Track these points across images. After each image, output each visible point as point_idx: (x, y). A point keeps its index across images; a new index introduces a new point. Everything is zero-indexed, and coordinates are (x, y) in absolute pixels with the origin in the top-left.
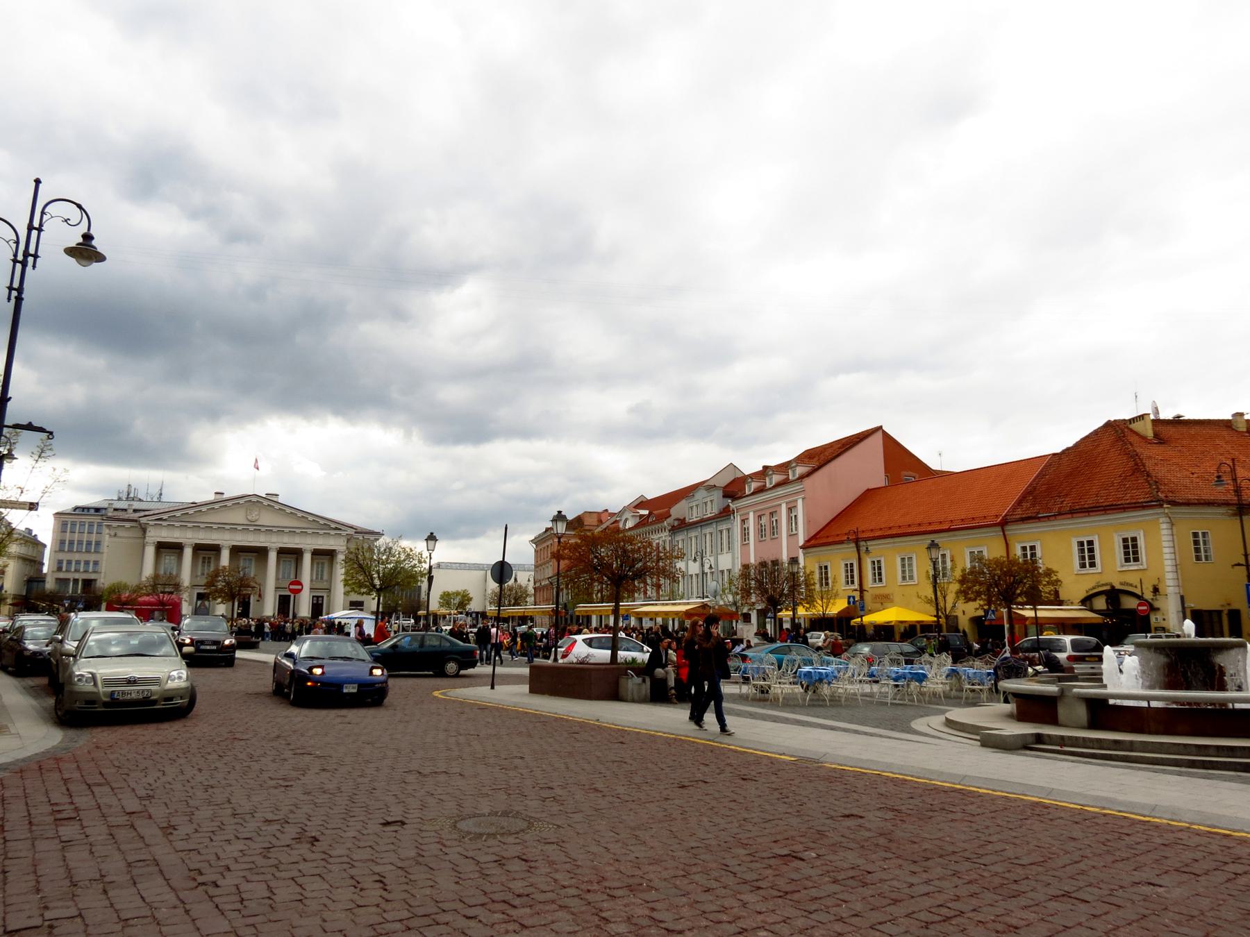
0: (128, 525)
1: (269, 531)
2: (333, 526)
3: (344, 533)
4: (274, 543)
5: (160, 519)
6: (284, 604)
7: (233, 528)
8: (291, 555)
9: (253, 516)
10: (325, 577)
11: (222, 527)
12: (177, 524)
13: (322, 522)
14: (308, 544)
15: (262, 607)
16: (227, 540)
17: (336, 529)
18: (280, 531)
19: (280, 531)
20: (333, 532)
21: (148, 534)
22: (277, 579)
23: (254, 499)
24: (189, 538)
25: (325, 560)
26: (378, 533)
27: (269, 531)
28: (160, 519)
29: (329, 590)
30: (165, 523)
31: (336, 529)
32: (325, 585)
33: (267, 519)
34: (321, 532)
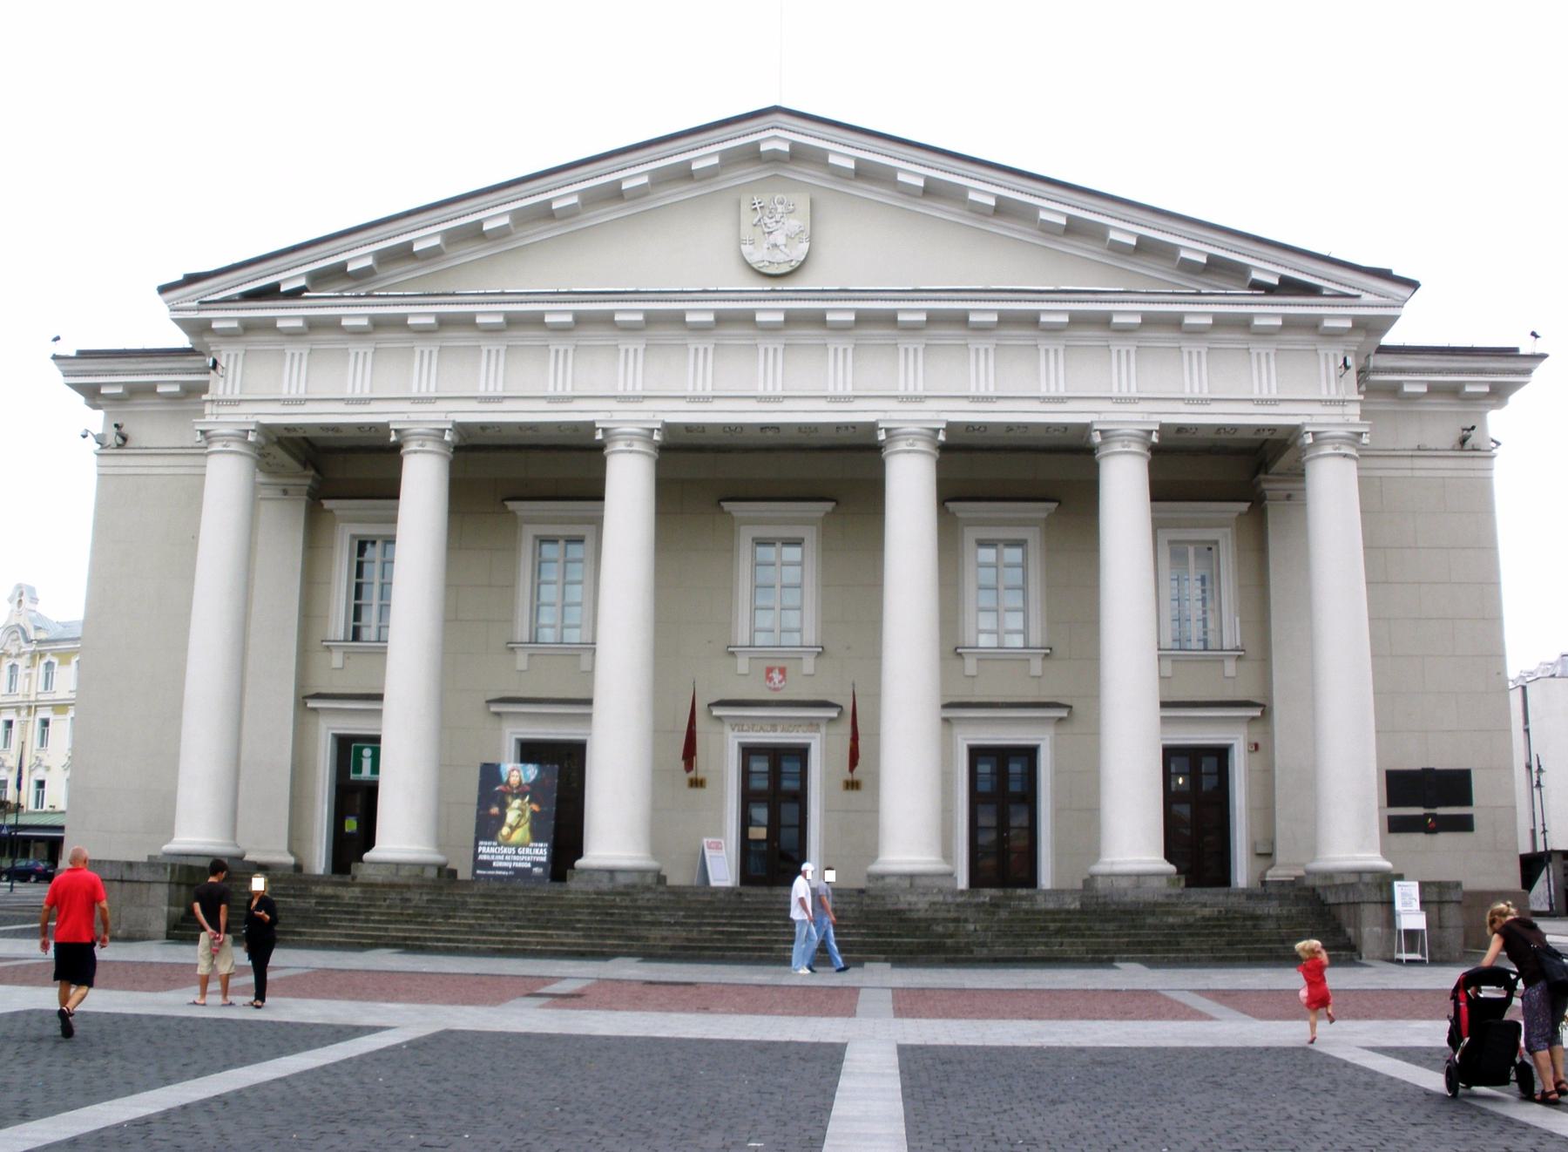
1: (876, 323)
2: (1267, 271)
3: (1337, 316)
4: (914, 398)
5: (270, 293)
6: (1002, 793)
9: (779, 243)
12: (355, 314)
14: (1124, 396)
15: (864, 830)
16: (630, 396)
17: (1289, 287)
20: (1269, 312)
21: (219, 387)
22: (952, 650)
23: (775, 140)
24: (421, 394)
25: (1219, 522)
26: (1510, 353)
27: (876, 323)
28: (270, 293)
29: (1259, 709)
30: (289, 315)
31: (1289, 287)
32: (1234, 680)
33: (867, 254)
34: (1199, 313)
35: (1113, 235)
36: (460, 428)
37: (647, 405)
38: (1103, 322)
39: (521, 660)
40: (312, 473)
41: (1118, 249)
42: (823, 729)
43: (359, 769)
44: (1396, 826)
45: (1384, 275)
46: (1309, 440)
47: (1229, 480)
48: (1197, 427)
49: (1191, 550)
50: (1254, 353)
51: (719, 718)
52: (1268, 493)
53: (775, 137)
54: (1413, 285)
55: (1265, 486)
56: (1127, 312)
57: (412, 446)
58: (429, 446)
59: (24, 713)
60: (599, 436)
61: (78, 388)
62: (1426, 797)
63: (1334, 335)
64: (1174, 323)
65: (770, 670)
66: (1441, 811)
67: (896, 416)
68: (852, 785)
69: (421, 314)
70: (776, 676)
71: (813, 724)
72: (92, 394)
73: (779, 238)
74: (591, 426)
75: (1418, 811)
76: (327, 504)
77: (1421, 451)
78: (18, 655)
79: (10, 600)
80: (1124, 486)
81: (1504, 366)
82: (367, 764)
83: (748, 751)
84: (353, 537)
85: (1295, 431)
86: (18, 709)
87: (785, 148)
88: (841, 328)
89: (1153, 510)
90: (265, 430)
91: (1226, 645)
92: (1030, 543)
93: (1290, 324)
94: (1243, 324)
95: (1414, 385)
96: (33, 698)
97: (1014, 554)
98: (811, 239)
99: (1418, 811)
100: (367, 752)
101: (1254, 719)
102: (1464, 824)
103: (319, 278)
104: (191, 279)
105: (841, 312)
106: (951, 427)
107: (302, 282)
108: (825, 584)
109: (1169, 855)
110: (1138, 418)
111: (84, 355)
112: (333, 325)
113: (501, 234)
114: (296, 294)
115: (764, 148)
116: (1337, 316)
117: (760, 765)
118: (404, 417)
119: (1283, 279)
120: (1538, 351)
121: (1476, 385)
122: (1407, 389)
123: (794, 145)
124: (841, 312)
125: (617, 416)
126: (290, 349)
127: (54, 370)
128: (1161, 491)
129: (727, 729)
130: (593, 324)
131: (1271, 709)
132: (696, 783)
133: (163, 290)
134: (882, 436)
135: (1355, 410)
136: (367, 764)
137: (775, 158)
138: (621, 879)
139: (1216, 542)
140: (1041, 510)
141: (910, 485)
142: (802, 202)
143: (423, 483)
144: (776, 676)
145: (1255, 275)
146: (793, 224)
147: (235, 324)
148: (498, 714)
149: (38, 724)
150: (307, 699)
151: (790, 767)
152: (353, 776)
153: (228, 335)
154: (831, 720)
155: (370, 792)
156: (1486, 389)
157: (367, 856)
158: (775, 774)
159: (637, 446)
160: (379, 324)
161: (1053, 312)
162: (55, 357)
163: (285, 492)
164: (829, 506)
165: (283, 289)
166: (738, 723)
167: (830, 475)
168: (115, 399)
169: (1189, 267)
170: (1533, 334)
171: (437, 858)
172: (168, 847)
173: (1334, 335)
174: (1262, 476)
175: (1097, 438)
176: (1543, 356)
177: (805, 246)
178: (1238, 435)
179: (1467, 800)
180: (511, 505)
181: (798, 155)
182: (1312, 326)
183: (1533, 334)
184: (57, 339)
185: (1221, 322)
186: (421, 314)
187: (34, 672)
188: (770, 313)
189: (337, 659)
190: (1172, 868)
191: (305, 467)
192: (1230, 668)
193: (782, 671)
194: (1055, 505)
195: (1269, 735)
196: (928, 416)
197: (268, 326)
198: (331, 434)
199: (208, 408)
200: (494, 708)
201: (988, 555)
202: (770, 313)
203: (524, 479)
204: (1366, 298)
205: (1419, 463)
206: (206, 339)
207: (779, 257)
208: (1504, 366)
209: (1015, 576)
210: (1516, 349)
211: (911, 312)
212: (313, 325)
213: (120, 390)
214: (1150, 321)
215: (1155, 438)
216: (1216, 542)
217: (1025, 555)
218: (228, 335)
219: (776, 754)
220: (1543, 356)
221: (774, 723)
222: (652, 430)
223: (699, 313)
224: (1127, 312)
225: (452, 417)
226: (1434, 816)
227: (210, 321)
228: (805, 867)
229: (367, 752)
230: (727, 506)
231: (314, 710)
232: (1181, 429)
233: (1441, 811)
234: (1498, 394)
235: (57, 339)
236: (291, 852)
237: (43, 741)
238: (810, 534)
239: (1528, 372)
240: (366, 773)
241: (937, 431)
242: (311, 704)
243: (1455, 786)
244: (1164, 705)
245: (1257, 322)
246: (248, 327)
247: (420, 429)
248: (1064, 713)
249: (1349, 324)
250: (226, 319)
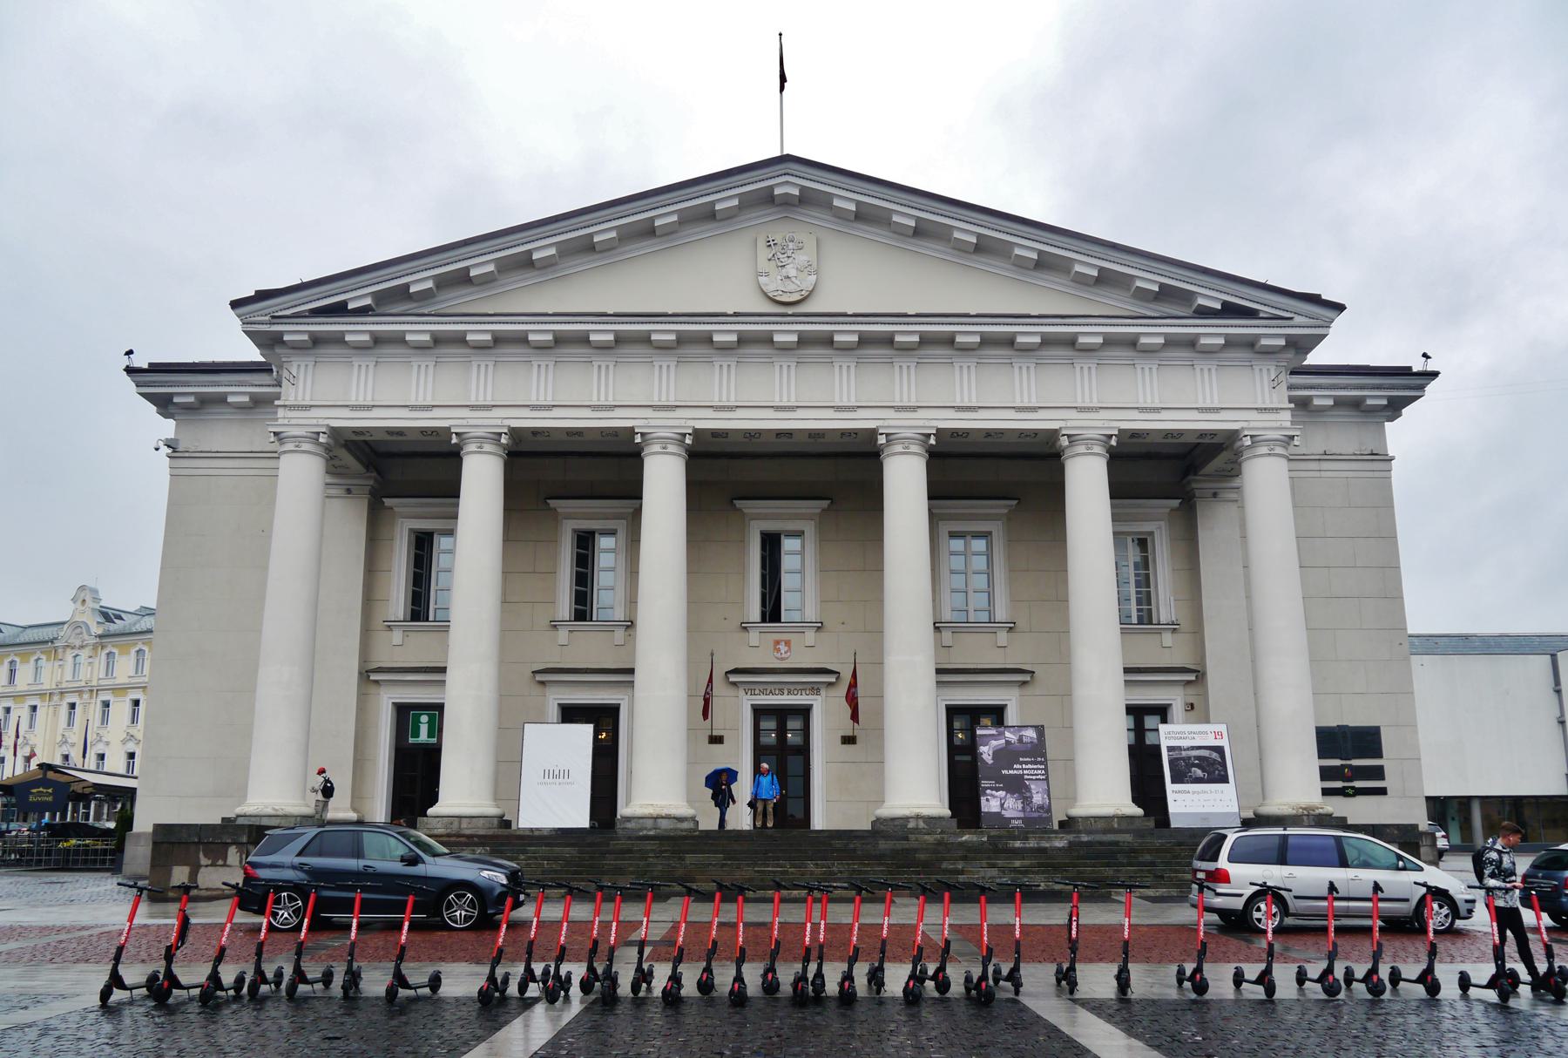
0: (238, 391)
1: (877, 342)
3: (1272, 335)
4: (906, 407)
5: (339, 310)
7: (693, 341)
8: (995, 481)
9: (788, 280)
10: (1167, 606)
11: (631, 340)
12: (418, 331)
13: (1149, 282)
14: (1089, 405)
16: (665, 407)
17: (1230, 311)
18: (938, 343)
19: (938, 343)
20: (1213, 333)
21: (289, 394)
23: (787, 187)
25: (1157, 520)
26: (1405, 372)
27: (877, 342)
28: (339, 310)
30: (357, 331)
32: (1169, 650)
34: (1152, 334)
35: (1078, 268)
36: (514, 433)
37: (679, 413)
38: (1070, 342)
39: (562, 635)
40: (374, 474)
41: (1081, 280)
42: (823, 692)
45: (1314, 299)
46: (1247, 442)
47: (1172, 477)
48: (1148, 432)
49: (1129, 539)
50: (1198, 368)
51: (734, 684)
52: (1197, 493)
53: (787, 183)
54: (1340, 308)
55: (1194, 485)
56: (1090, 334)
57: (472, 447)
58: (487, 447)
59: (86, 696)
60: (638, 439)
61: (149, 397)
62: (1350, 752)
63: (1269, 352)
64: (1132, 343)
65: (777, 643)
67: (892, 423)
68: (849, 740)
69: (478, 333)
70: (783, 648)
71: (815, 689)
72: (164, 404)
73: (792, 272)
74: (631, 431)
75: (1337, 762)
76: (388, 502)
77: (1326, 457)
78: (82, 647)
79: (74, 600)
80: (1087, 484)
81: (1402, 385)
82: (424, 729)
83: (759, 712)
84: (411, 530)
85: (1233, 435)
86: (80, 692)
87: (796, 192)
88: (846, 348)
89: (1113, 506)
90: (335, 432)
91: (1163, 620)
92: (995, 534)
93: (1231, 343)
94: (1191, 343)
95: (1322, 399)
96: (94, 683)
97: (979, 545)
98: (817, 272)
99: (1337, 762)
100: (424, 719)
101: (1189, 682)
103: (380, 297)
104: (262, 295)
105: (846, 335)
106: (940, 433)
107: (368, 301)
108: (822, 570)
109: (1136, 800)
110: (1099, 424)
111: (156, 368)
112: (399, 340)
113: (548, 264)
114: (363, 311)
115: (777, 191)
116: (1272, 335)
117: (769, 724)
118: (464, 422)
119: (1225, 304)
120: (1430, 368)
121: (1376, 398)
122: (1316, 402)
123: (803, 189)
124: (846, 335)
125: (653, 422)
126: (356, 361)
127: (128, 382)
128: (1119, 490)
129: (742, 692)
130: (631, 340)
131: (1204, 674)
132: (716, 740)
133: (235, 304)
134: (882, 440)
135: (1287, 416)
136: (424, 729)
137: (787, 203)
138: (665, 824)
139: (1152, 533)
140: (1001, 507)
141: (905, 483)
142: (810, 243)
143: (482, 479)
144: (783, 648)
145: (1201, 301)
146: (802, 258)
147: (306, 337)
148: (542, 683)
149: (99, 705)
150: (369, 676)
151: (794, 724)
152: (411, 740)
153: (297, 347)
154: (830, 684)
155: (432, 755)
156: (1385, 402)
157: (430, 811)
158: (782, 731)
159: (672, 448)
160: (438, 340)
161: (1028, 335)
162: (130, 370)
163: (349, 491)
164: (825, 503)
165: (351, 306)
166: (750, 688)
167: (837, 476)
168: (187, 408)
169: (1142, 295)
170: (1425, 355)
171: (492, 811)
172: (239, 810)
173: (1269, 352)
174: (1191, 477)
175: (1064, 442)
176: (1434, 375)
177: (814, 278)
178: (1182, 440)
179: (1380, 756)
180: (552, 503)
181: (806, 199)
182: (1250, 344)
183: (1425, 355)
185: (1172, 342)
186: (478, 333)
187: (96, 661)
188: (786, 334)
189: (397, 636)
190: (1140, 811)
191: (367, 467)
192: (1168, 639)
193: (788, 643)
194: (1014, 502)
195: (1205, 696)
196: (921, 423)
197: (338, 340)
198: (394, 438)
199: (281, 413)
200: (539, 677)
201: (957, 545)
202: (786, 334)
203: (571, 480)
204: (1298, 320)
205: (1325, 465)
206: (278, 350)
207: (791, 287)
208: (1402, 385)
209: (980, 563)
210: (1410, 368)
211: (907, 334)
212: (378, 340)
213: (191, 399)
214: (1110, 342)
215: (1113, 442)
216: (1152, 533)
217: (990, 546)
218: (297, 347)
219: (781, 714)
220: (1435, 374)
221: (781, 688)
222: (684, 435)
223: (725, 334)
224: (1090, 334)
225: (507, 422)
226: (1350, 767)
227: (281, 333)
228: (954, 822)
229: (424, 719)
230: (738, 503)
231: (376, 682)
232: (1135, 434)
234: (1394, 408)
235: (130, 353)
236: (354, 810)
237: (105, 718)
238: (809, 528)
239: (1422, 388)
240: (423, 737)
241: (929, 436)
242: (373, 677)
243: (1366, 741)
244: (1127, 671)
245: (1203, 341)
246: (317, 341)
247: (480, 432)
248: (1027, 678)
249: (1282, 342)
250: (295, 332)
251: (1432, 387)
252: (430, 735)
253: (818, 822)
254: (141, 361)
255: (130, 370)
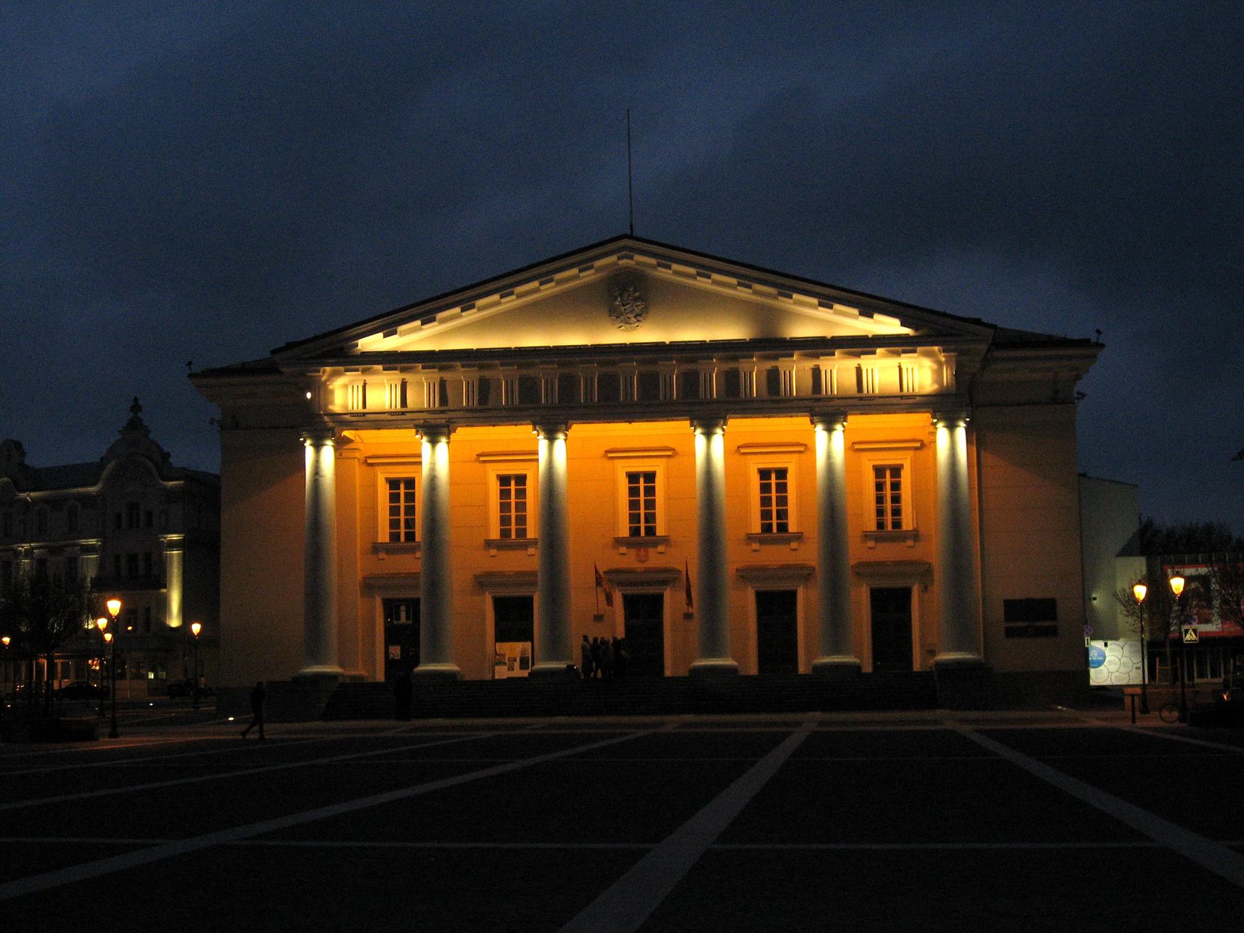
26: (1084, 343)
43: (398, 618)
44: (1010, 633)
45: (977, 322)
66: (1038, 624)
75: (1024, 624)
82: (403, 615)
99: (1024, 624)
100: (403, 608)
102: (1052, 632)
120: (1101, 341)
136: (403, 615)
170: (1098, 332)
176: (1103, 346)
179: (1054, 618)
183: (1098, 332)
184: (190, 363)
220: (1103, 346)
229: (403, 608)
233: (1038, 624)
235: (190, 363)
239: (1095, 357)
251: (1103, 354)
252: (407, 618)
253: (668, 673)
254: (197, 369)
255: (190, 376)
